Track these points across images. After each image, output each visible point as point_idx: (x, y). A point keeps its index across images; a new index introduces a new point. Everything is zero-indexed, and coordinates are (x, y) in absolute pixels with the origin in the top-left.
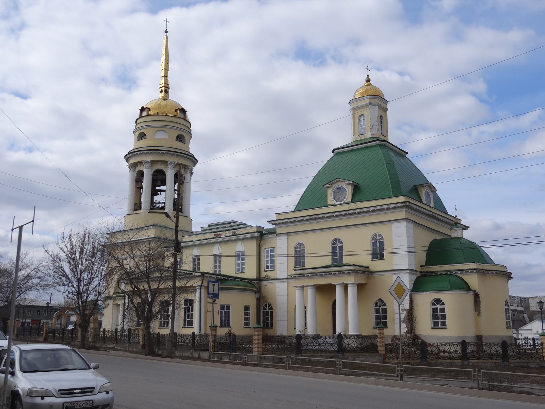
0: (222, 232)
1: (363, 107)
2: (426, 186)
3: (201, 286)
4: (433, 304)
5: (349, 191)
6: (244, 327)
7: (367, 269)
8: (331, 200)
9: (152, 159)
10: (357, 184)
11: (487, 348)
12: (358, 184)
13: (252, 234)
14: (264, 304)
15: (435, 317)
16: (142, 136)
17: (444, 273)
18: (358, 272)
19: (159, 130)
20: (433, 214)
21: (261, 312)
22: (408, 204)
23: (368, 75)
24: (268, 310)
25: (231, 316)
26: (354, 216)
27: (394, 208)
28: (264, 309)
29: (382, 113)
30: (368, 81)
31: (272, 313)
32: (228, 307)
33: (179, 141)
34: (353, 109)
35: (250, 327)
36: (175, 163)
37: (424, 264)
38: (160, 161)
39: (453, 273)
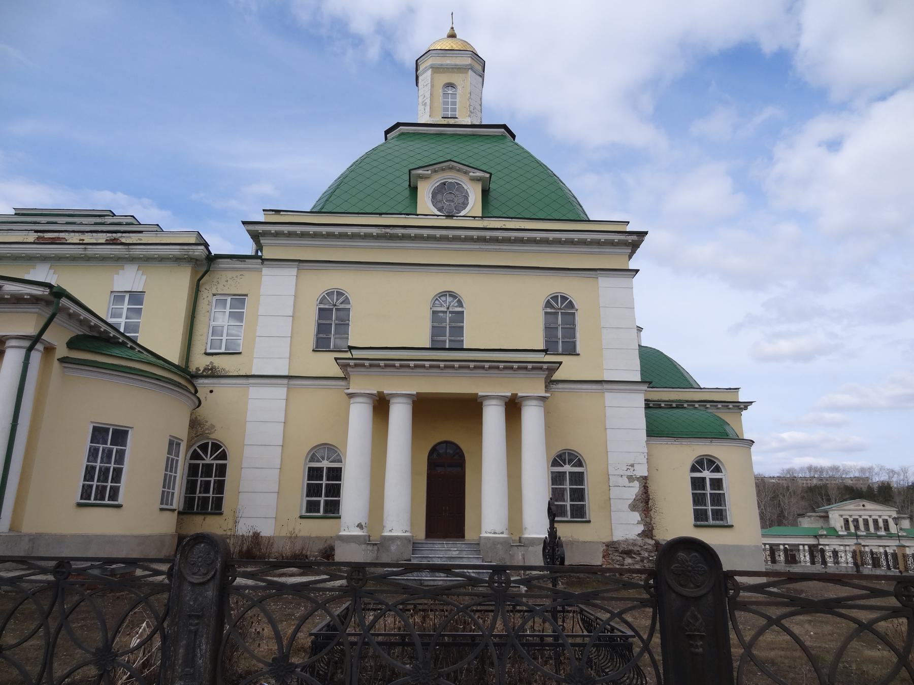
0: (67, 234)
1: (455, 70)
3: (36, 339)
6: (161, 510)
8: (425, 202)
13: (186, 247)
14: (199, 444)
15: (698, 499)
17: (674, 405)
24: (208, 461)
25: (126, 467)
26: (498, 247)
31: (222, 470)
32: (120, 436)
34: (432, 68)
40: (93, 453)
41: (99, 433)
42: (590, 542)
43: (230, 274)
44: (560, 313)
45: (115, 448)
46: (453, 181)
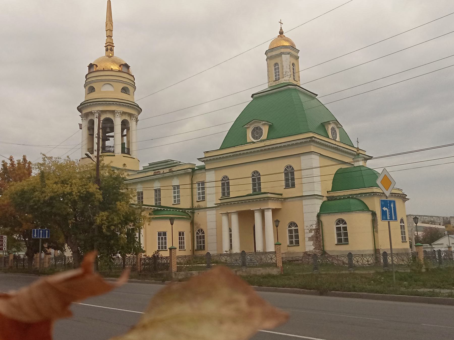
2: (332, 123)
4: (337, 224)
5: (265, 130)
7: (280, 197)
8: (250, 138)
9: (101, 109)
10: (271, 124)
11: (360, 259)
12: (272, 123)
13: (185, 170)
14: (198, 230)
15: (339, 235)
16: (92, 90)
18: (272, 199)
19: (105, 84)
20: (338, 147)
21: (195, 236)
22: (313, 139)
23: (281, 28)
27: (301, 143)
28: (197, 233)
29: (293, 61)
30: (281, 33)
31: (204, 236)
33: (125, 93)
35: (185, 249)
36: (122, 112)
37: (331, 190)
39: (354, 196)
40: (159, 238)
41: (159, 234)
42: (300, 252)
43: (200, 175)
44: (289, 173)
45: (164, 237)
46: (253, 128)
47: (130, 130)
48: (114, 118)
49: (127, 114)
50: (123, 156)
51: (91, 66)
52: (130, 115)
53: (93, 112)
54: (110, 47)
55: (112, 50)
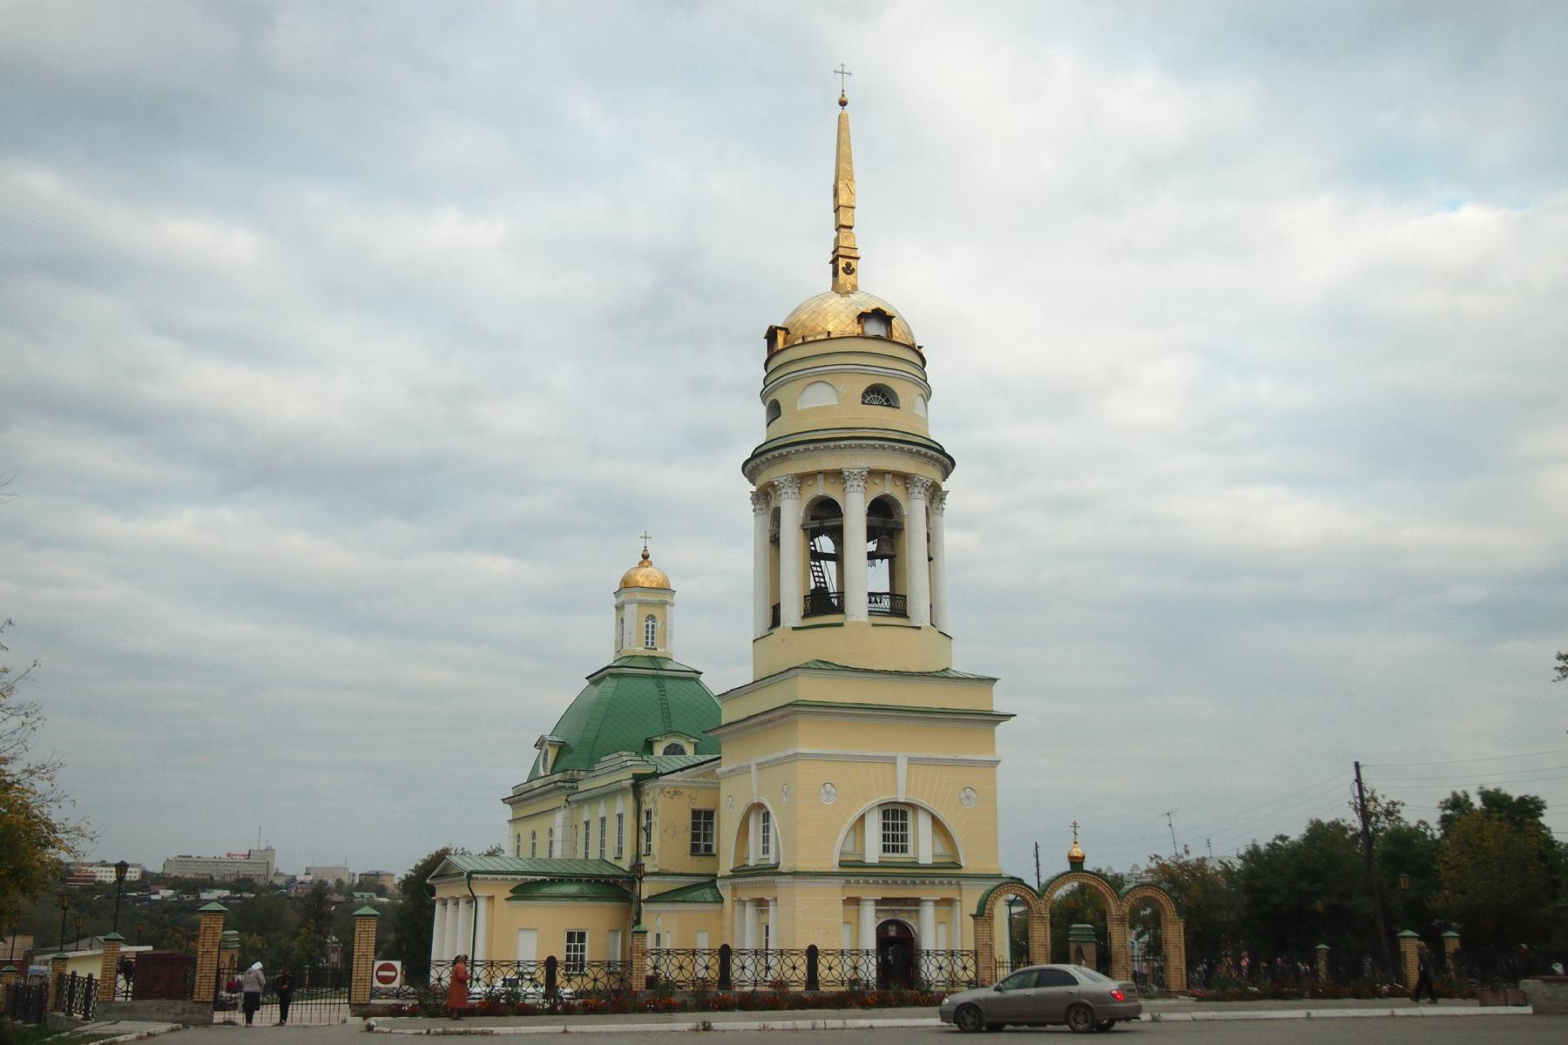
16: (774, 410)
36: (865, 473)
38: (820, 472)
47: (906, 530)
48: (845, 495)
49: (889, 477)
50: (873, 625)
51: (772, 335)
52: (905, 478)
53: (776, 483)
54: (843, 263)
55: (849, 270)
